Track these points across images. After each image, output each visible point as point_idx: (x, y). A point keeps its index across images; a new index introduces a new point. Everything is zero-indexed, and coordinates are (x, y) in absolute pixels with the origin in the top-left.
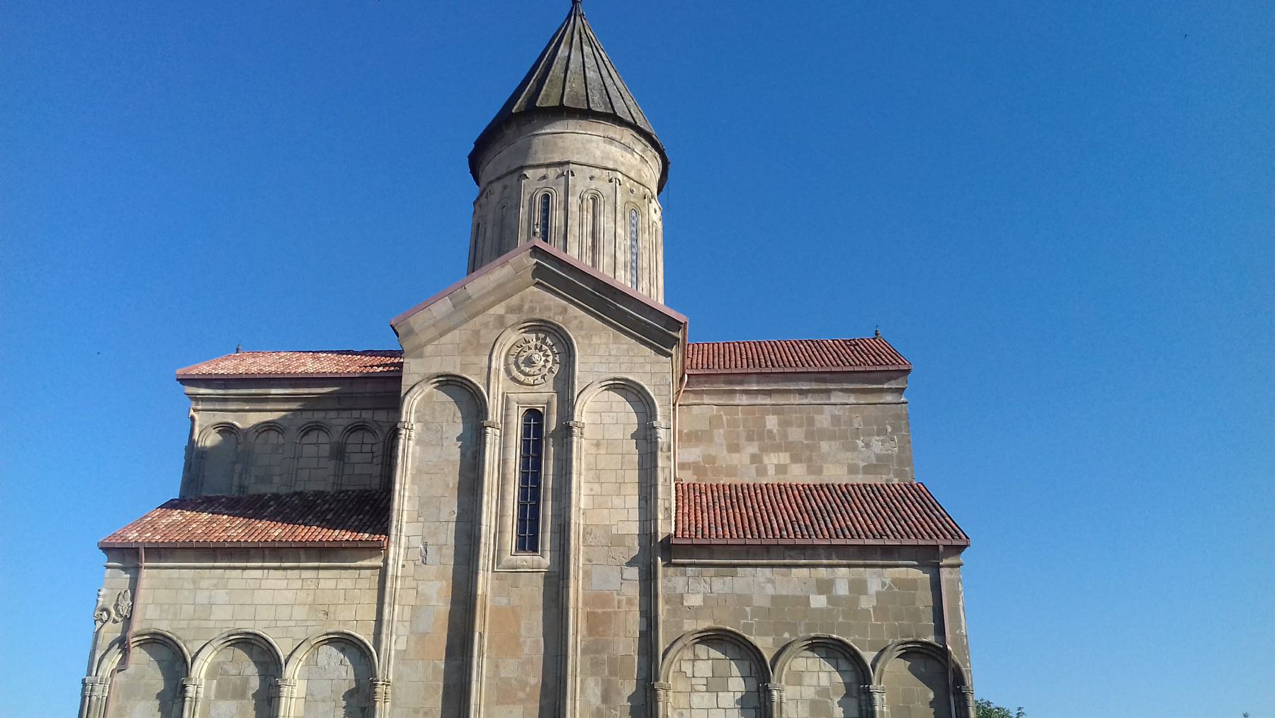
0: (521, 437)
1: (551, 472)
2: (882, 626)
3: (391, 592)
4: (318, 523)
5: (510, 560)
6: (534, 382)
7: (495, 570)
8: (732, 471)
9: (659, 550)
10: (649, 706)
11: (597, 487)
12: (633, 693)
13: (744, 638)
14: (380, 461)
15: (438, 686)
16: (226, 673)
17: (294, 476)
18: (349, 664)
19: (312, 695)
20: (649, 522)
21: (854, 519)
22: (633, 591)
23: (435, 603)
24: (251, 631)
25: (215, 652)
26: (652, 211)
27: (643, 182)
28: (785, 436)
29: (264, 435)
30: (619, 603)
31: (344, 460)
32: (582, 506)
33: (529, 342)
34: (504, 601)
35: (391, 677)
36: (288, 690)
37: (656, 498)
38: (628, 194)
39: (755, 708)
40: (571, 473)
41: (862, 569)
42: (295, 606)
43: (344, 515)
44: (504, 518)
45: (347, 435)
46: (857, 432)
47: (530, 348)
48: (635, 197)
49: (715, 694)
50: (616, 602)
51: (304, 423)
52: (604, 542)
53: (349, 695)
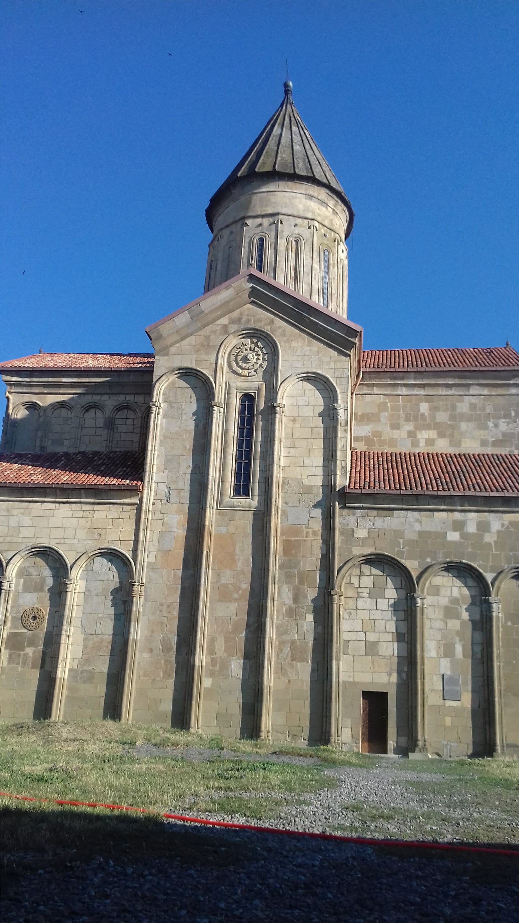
0: (239, 414)
1: (260, 439)
2: (500, 554)
3: (145, 522)
4: (94, 472)
5: (229, 501)
6: (249, 373)
7: (219, 508)
9: (337, 497)
10: (327, 606)
11: (293, 451)
12: (316, 597)
13: (397, 561)
15: (177, 587)
16: (29, 574)
18: (115, 570)
19: (89, 591)
20: (330, 477)
22: (317, 526)
24: (47, 545)
25: (22, 559)
26: (340, 251)
27: (334, 228)
30: (307, 534)
32: (282, 464)
33: (246, 345)
34: (224, 530)
35: (144, 580)
36: (73, 587)
37: (336, 460)
38: (322, 237)
39: (404, 611)
40: (274, 440)
41: (487, 514)
43: (113, 467)
44: (225, 471)
45: (115, 412)
46: (488, 417)
47: (246, 350)
48: (328, 240)
49: (375, 600)
50: (305, 533)
52: (297, 490)
53: (115, 592)
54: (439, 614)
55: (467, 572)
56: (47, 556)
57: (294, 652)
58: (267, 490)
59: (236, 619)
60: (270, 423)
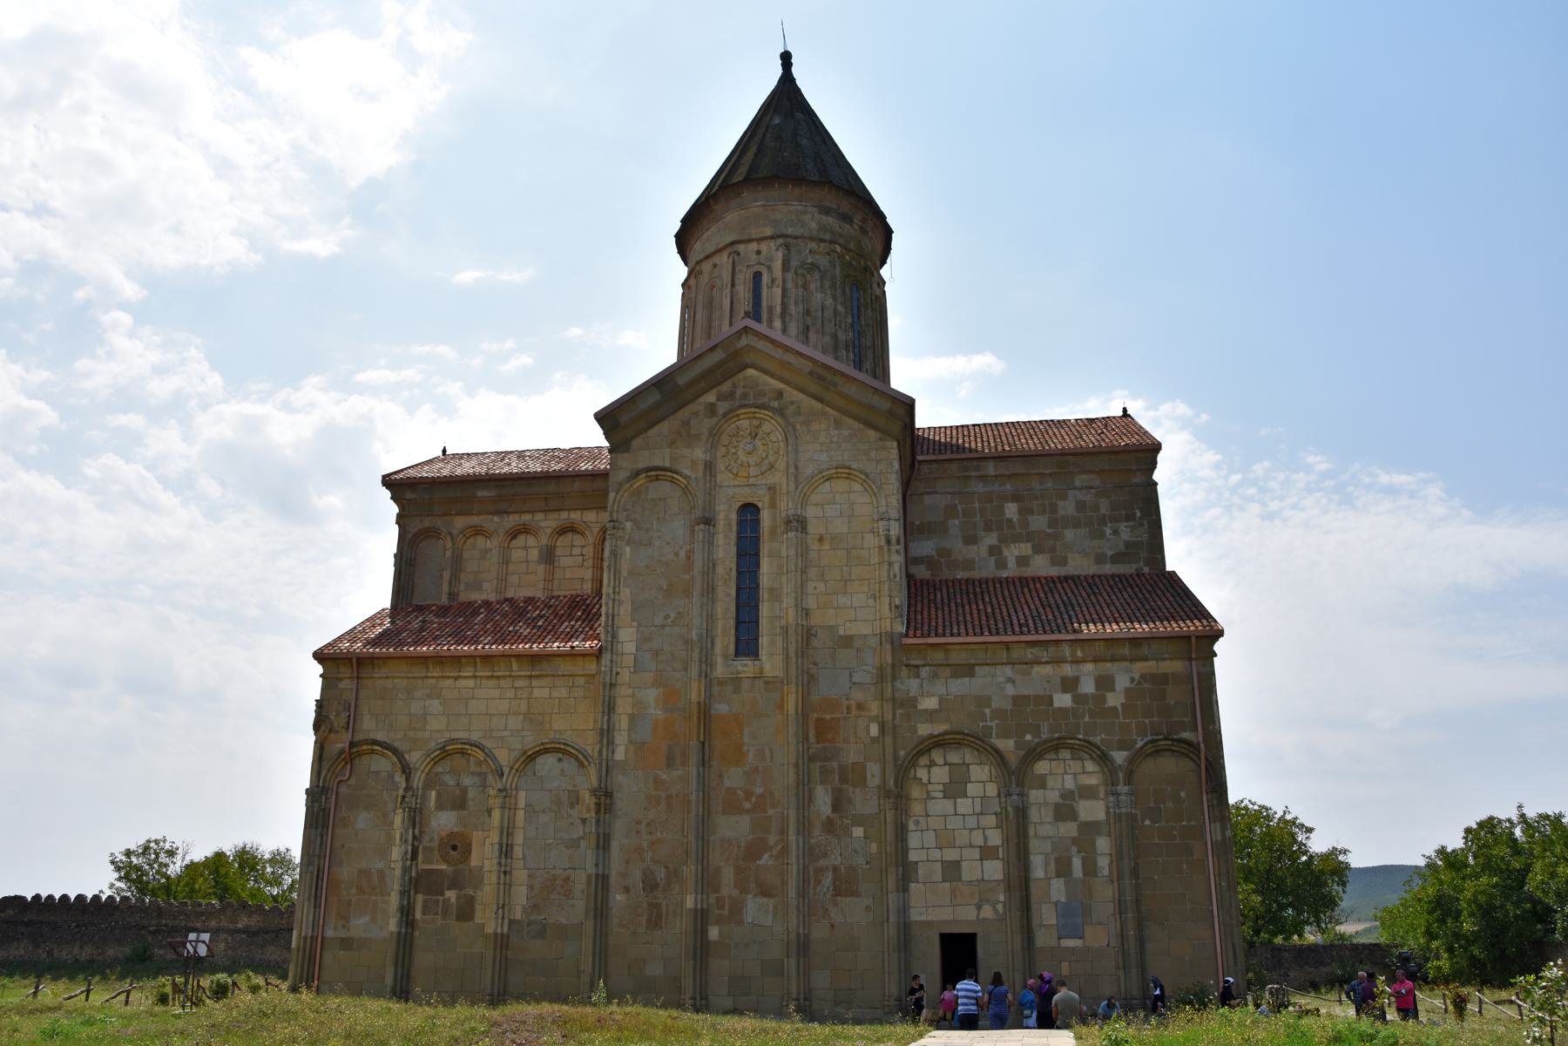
2: (1132, 722)
8: (969, 564)
14: (591, 565)
17: (504, 582)
19: (531, 805)
21: (1100, 612)
23: (653, 712)
24: (466, 741)
28: (1025, 524)
29: (472, 540)
31: (553, 564)
39: (996, 814)
42: (509, 716)
43: (555, 621)
46: (1103, 521)
51: (511, 526)
54: (1048, 815)
55: (1084, 752)
56: (468, 757)
57: (837, 883)
58: (785, 646)
59: (749, 838)
60: (785, 546)
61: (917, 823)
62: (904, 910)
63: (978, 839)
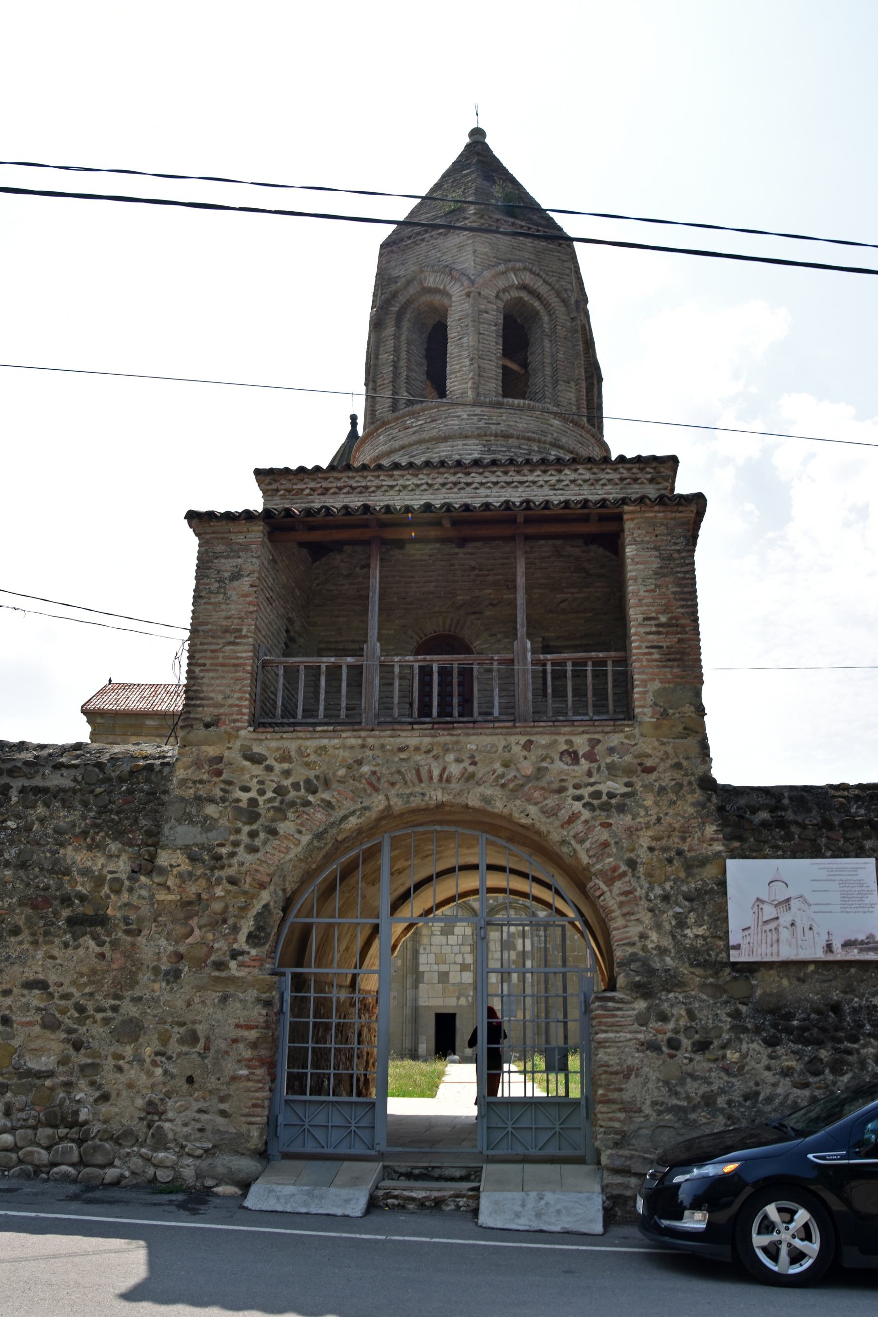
61: (425, 949)
62: (416, 999)
63: (459, 959)
